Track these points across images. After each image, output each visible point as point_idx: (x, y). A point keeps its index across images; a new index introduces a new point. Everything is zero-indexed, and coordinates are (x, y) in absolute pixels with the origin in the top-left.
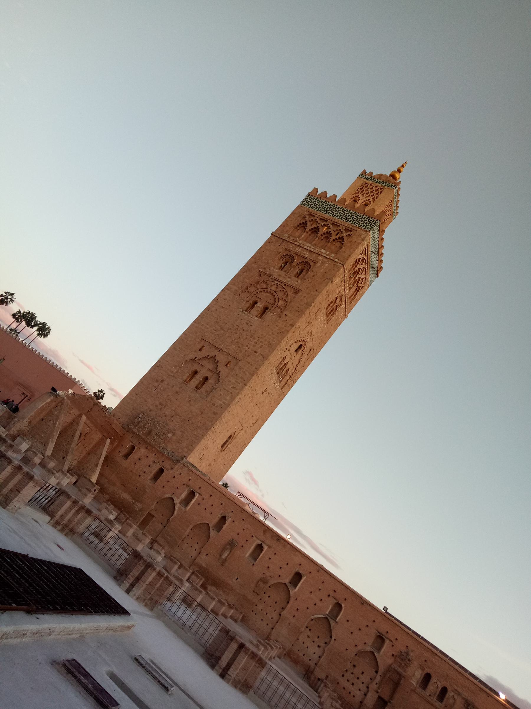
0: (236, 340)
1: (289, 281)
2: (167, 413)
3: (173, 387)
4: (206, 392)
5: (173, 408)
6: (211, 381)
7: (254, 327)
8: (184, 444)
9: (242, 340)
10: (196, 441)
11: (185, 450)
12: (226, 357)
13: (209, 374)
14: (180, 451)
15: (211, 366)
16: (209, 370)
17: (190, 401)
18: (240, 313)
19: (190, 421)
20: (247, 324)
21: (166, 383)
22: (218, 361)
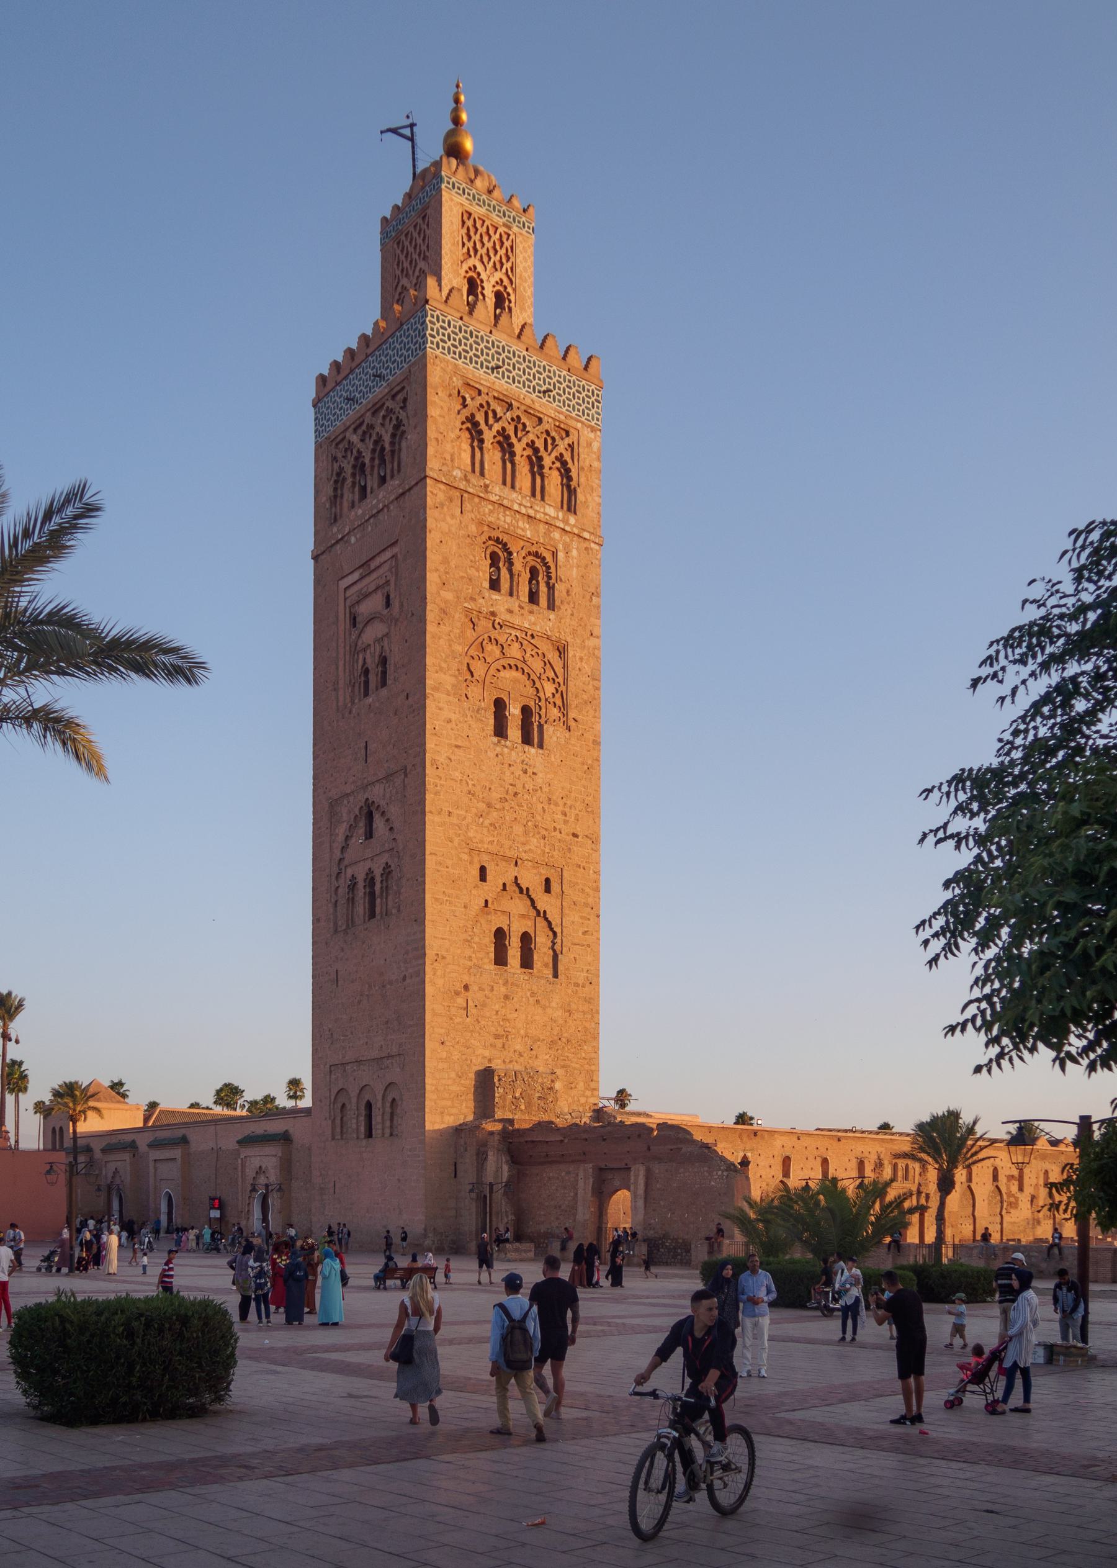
0: (530, 824)
1: (534, 624)
2: (518, 1047)
3: (492, 989)
4: (546, 965)
5: (522, 1032)
6: (542, 941)
7: (540, 775)
8: (581, 1086)
9: (539, 818)
10: (593, 1068)
11: (588, 1093)
12: (535, 871)
13: (527, 926)
14: (583, 1100)
15: (519, 906)
16: (522, 916)
17: (538, 1001)
18: (498, 749)
19: (564, 1040)
20: (525, 772)
21: (474, 988)
22: (528, 889)
